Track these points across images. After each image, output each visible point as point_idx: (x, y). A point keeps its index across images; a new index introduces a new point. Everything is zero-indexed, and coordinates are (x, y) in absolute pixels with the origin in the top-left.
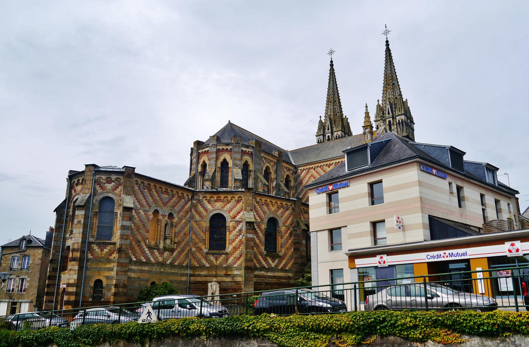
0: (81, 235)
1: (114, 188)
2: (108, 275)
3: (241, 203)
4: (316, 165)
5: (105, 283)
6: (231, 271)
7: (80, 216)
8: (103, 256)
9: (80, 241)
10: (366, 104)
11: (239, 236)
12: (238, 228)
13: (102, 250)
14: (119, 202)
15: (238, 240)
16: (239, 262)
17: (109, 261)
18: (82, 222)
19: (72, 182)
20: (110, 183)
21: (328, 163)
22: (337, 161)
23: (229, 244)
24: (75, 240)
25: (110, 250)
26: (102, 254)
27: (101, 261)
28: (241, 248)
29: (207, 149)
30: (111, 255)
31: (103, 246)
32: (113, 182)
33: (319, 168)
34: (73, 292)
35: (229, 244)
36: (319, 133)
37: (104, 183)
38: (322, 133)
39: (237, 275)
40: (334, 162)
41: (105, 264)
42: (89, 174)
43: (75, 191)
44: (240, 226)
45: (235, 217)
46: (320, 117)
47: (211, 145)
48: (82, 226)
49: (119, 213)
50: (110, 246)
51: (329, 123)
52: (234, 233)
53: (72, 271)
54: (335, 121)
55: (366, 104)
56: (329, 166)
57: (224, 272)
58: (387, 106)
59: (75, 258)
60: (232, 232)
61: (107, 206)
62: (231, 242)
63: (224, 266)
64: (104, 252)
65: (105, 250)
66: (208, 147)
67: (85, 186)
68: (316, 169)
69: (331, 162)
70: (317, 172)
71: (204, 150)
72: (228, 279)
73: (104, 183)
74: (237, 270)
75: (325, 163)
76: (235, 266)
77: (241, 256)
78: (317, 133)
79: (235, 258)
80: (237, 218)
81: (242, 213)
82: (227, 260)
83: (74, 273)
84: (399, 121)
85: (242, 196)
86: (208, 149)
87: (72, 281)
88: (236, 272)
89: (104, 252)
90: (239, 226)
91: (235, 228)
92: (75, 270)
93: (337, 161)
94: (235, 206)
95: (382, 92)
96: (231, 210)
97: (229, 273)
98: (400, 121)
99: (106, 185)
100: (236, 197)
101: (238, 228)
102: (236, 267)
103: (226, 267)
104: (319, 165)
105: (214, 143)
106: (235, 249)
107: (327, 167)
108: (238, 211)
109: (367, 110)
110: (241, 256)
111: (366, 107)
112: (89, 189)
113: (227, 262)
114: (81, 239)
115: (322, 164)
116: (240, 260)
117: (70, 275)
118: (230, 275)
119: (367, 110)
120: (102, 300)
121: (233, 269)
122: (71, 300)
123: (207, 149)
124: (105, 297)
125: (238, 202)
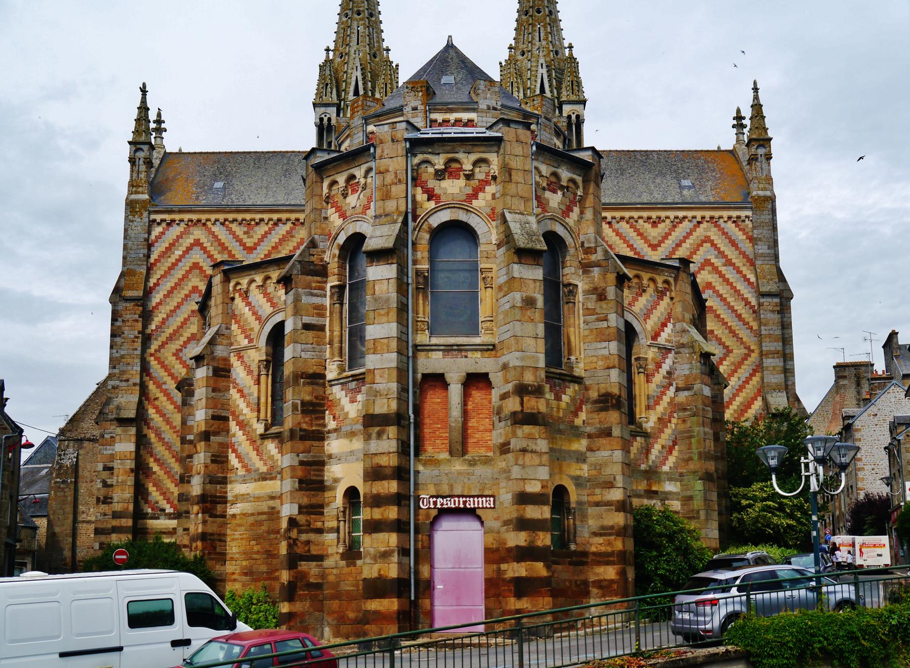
0: (541, 343)
1: (564, 208)
2: (578, 473)
3: (667, 299)
4: (618, 214)
5: (574, 496)
6: (659, 482)
7: (532, 285)
8: (561, 415)
9: (542, 364)
10: (755, 83)
11: (668, 389)
12: (666, 367)
13: (558, 398)
14: (582, 256)
15: (666, 399)
16: (672, 460)
17: (576, 432)
18: (540, 303)
19: (416, 160)
20: (555, 192)
21: (654, 214)
22: (681, 214)
23: (648, 408)
24: (523, 359)
25: (573, 399)
26: (558, 408)
27: (560, 432)
28: (674, 421)
29: (465, 116)
30: (577, 416)
31: (559, 385)
32: (562, 188)
33: (623, 224)
34: (545, 520)
35: (648, 408)
36: (326, 99)
37: (544, 189)
38: (335, 99)
39: (670, 493)
40: (672, 214)
41: (570, 441)
42: (518, 150)
43: (431, 195)
44: (669, 362)
45: (656, 336)
46: (328, 50)
47: (483, 106)
48: (538, 316)
49: (580, 290)
50: (572, 385)
51: (359, 73)
52: (658, 378)
53: (528, 455)
54: (354, 74)
55: (755, 83)
56: (655, 224)
57: (642, 486)
58: (540, 71)
59: (532, 415)
60: (653, 375)
61: (454, 253)
62: (652, 402)
63: (643, 467)
64: (563, 405)
65: (564, 396)
66: (474, 110)
67: (512, 188)
68: (616, 226)
69: (663, 214)
70: (618, 234)
71: (452, 117)
72: (656, 504)
73: (544, 189)
74: (670, 480)
75: (645, 214)
76: (666, 468)
77: (675, 443)
78: (319, 94)
79: (663, 447)
80: (662, 340)
81: (670, 326)
82: (648, 452)
83: (537, 460)
84: (569, 117)
85: (671, 280)
86: (472, 116)
87: (534, 488)
88: (670, 487)
89: (563, 405)
90: (667, 361)
91: (659, 366)
92: (540, 454)
93: (681, 214)
94: (654, 306)
95: (515, 25)
96: (647, 316)
97: (654, 488)
98: (574, 117)
99: (548, 194)
100: (660, 280)
101: (666, 367)
102: (667, 473)
103: (646, 472)
104: (627, 214)
105: (493, 103)
106: (663, 422)
107: (648, 226)
108: (663, 321)
109: (756, 98)
110: (675, 443)
111: (756, 89)
112: (526, 200)
113: (647, 458)
114: (542, 357)
115: (635, 214)
116: (675, 453)
117: (523, 466)
118: (656, 492)
119: (756, 98)
120: (573, 547)
121: (663, 476)
122: (539, 543)
123: (465, 116)
124: (579, 540)
125: (661, 294)
